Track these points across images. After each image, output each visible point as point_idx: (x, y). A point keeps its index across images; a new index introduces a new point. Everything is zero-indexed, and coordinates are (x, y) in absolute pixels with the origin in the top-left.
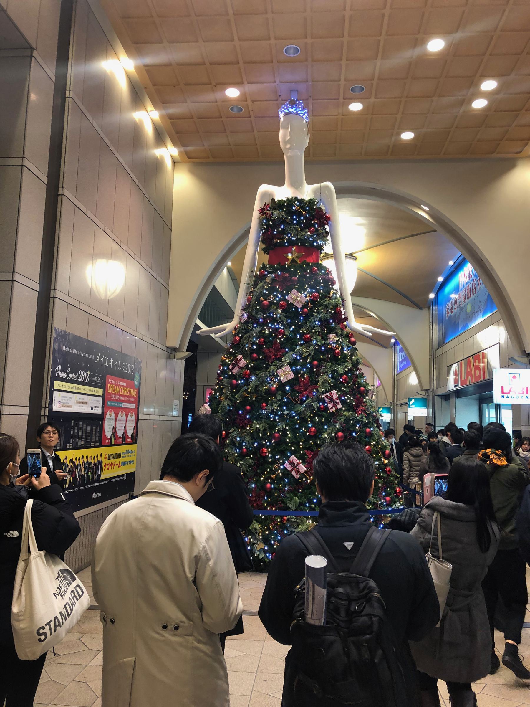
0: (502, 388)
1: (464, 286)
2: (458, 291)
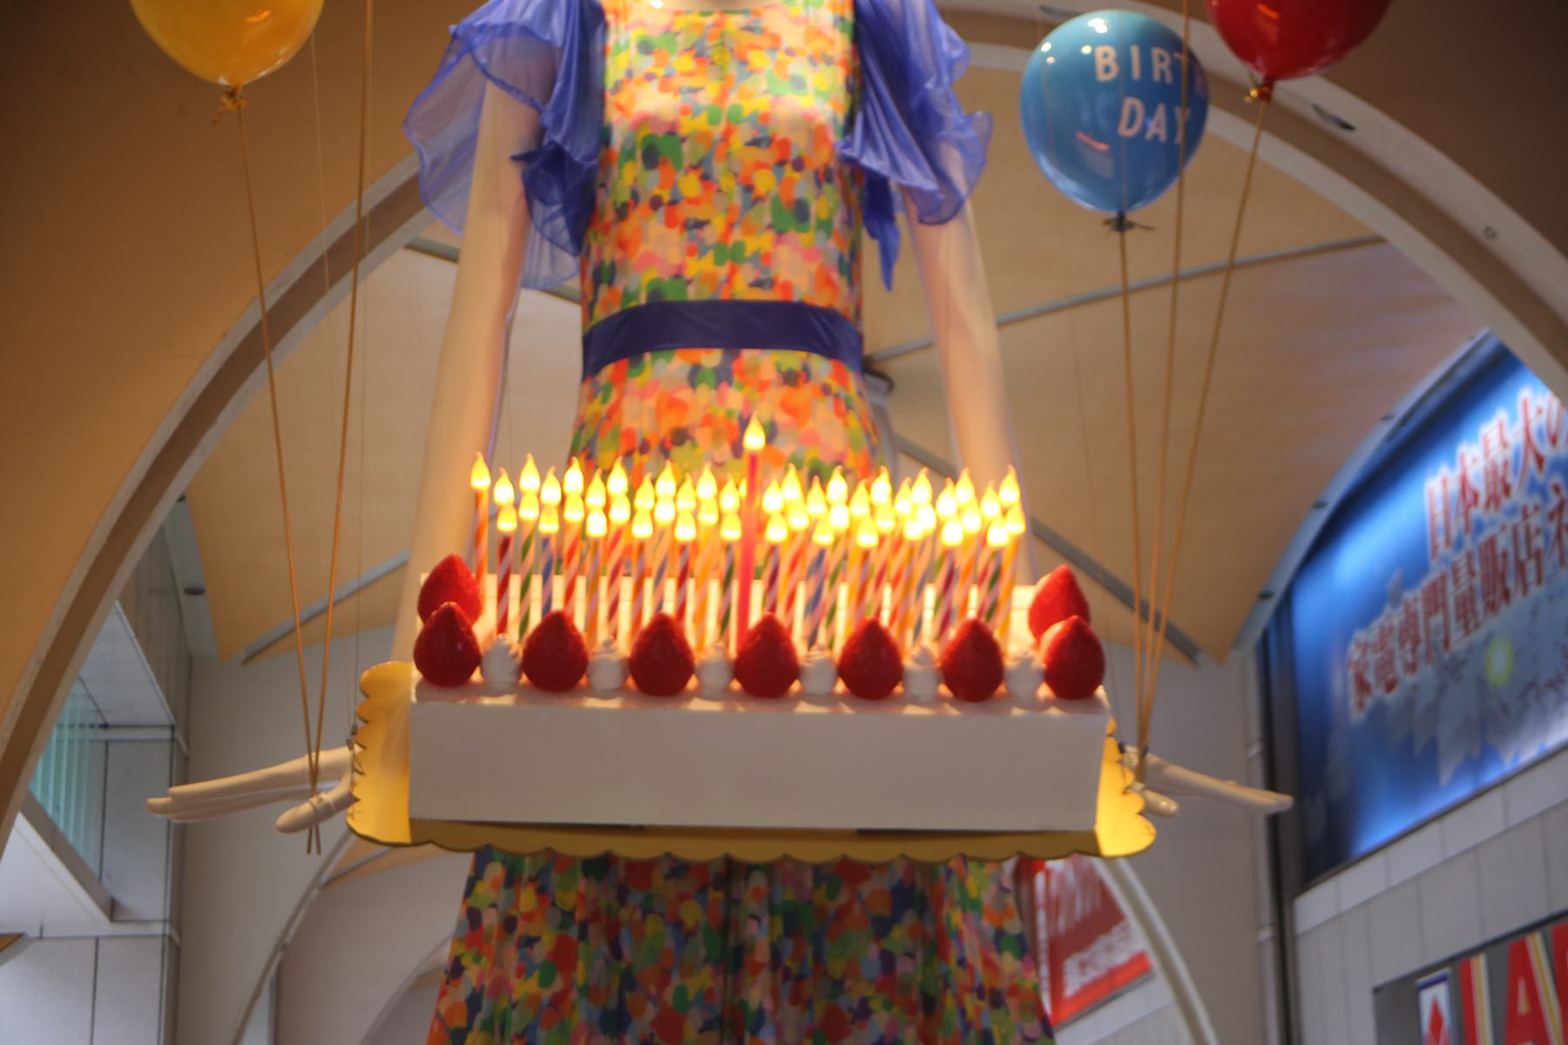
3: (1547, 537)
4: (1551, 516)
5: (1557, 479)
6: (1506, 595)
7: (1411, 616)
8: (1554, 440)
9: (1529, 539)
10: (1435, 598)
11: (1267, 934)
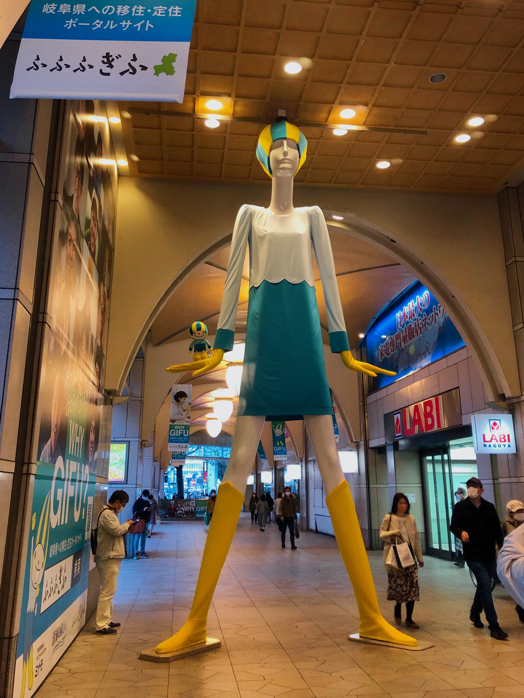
0: (484, 435)
1: (403, 326)
2: (396, 331)
5: (425, 313)
6: (414, 336)
7: (392, 340)
8: (424, 306)
10: (398, 337)
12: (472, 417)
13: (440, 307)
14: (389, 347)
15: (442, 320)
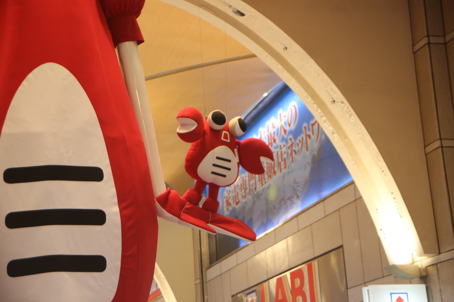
3: (288, 154)
4: (289, 148)
5: (291, 136)
6: (275, 173)
8: (289, 125)
9: (282, 155)
11: (198, 281)
12: (365, 290)
13: (313, 125)
14: (239, 191)
15: (316, 146)
